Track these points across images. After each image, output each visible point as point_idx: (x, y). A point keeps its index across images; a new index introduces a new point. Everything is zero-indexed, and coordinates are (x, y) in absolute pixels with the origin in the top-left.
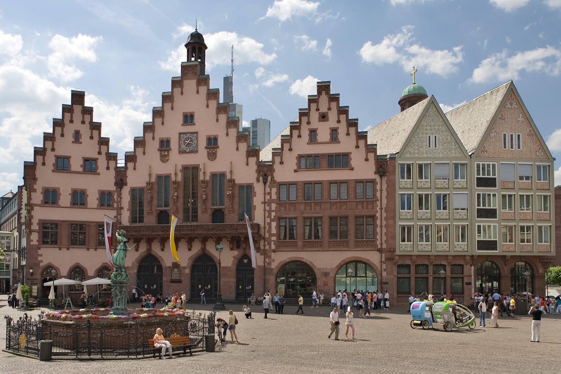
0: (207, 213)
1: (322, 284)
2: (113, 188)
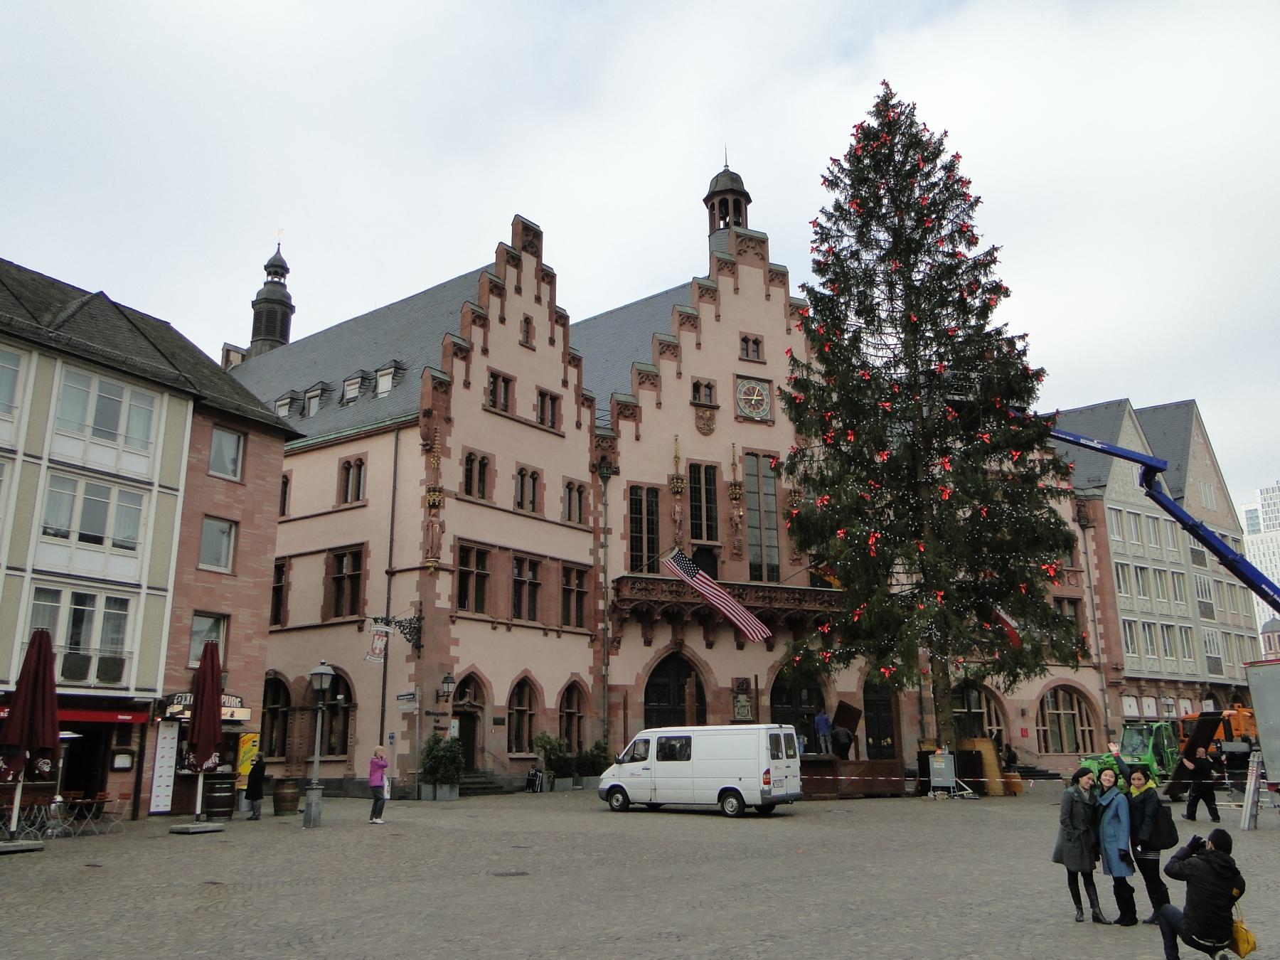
0: (801, 564)
1: (1019, 734)
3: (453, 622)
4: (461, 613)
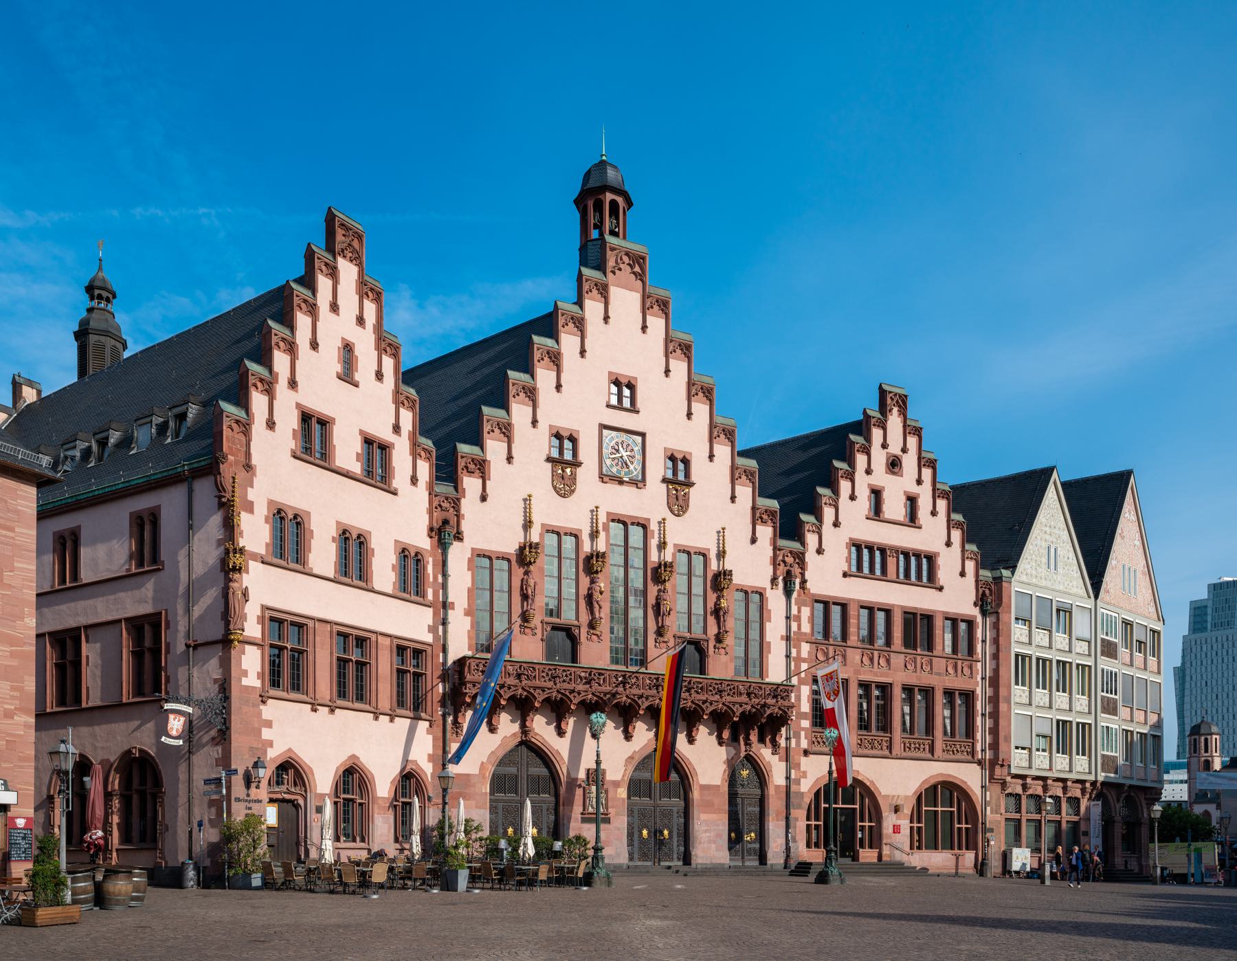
2: (423, 542)
3: (264, 702)
4: (273, 692)
